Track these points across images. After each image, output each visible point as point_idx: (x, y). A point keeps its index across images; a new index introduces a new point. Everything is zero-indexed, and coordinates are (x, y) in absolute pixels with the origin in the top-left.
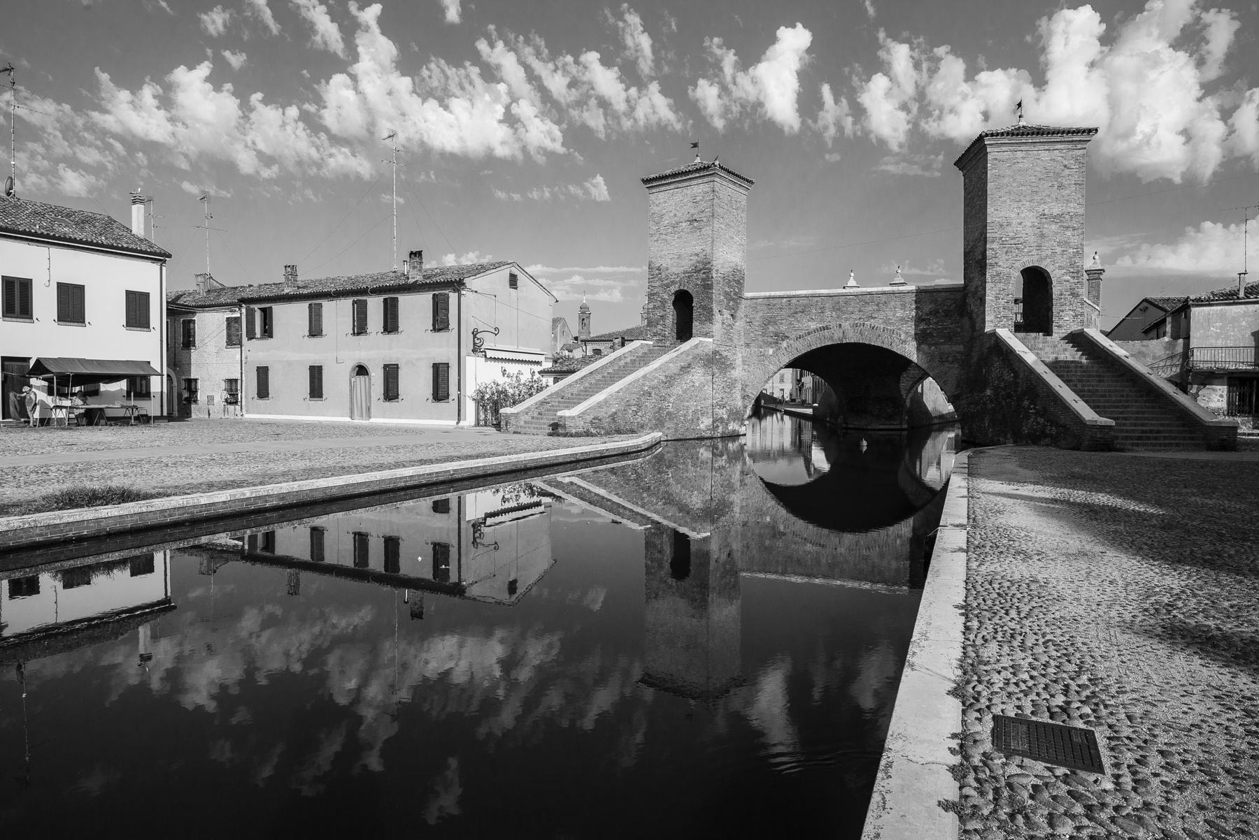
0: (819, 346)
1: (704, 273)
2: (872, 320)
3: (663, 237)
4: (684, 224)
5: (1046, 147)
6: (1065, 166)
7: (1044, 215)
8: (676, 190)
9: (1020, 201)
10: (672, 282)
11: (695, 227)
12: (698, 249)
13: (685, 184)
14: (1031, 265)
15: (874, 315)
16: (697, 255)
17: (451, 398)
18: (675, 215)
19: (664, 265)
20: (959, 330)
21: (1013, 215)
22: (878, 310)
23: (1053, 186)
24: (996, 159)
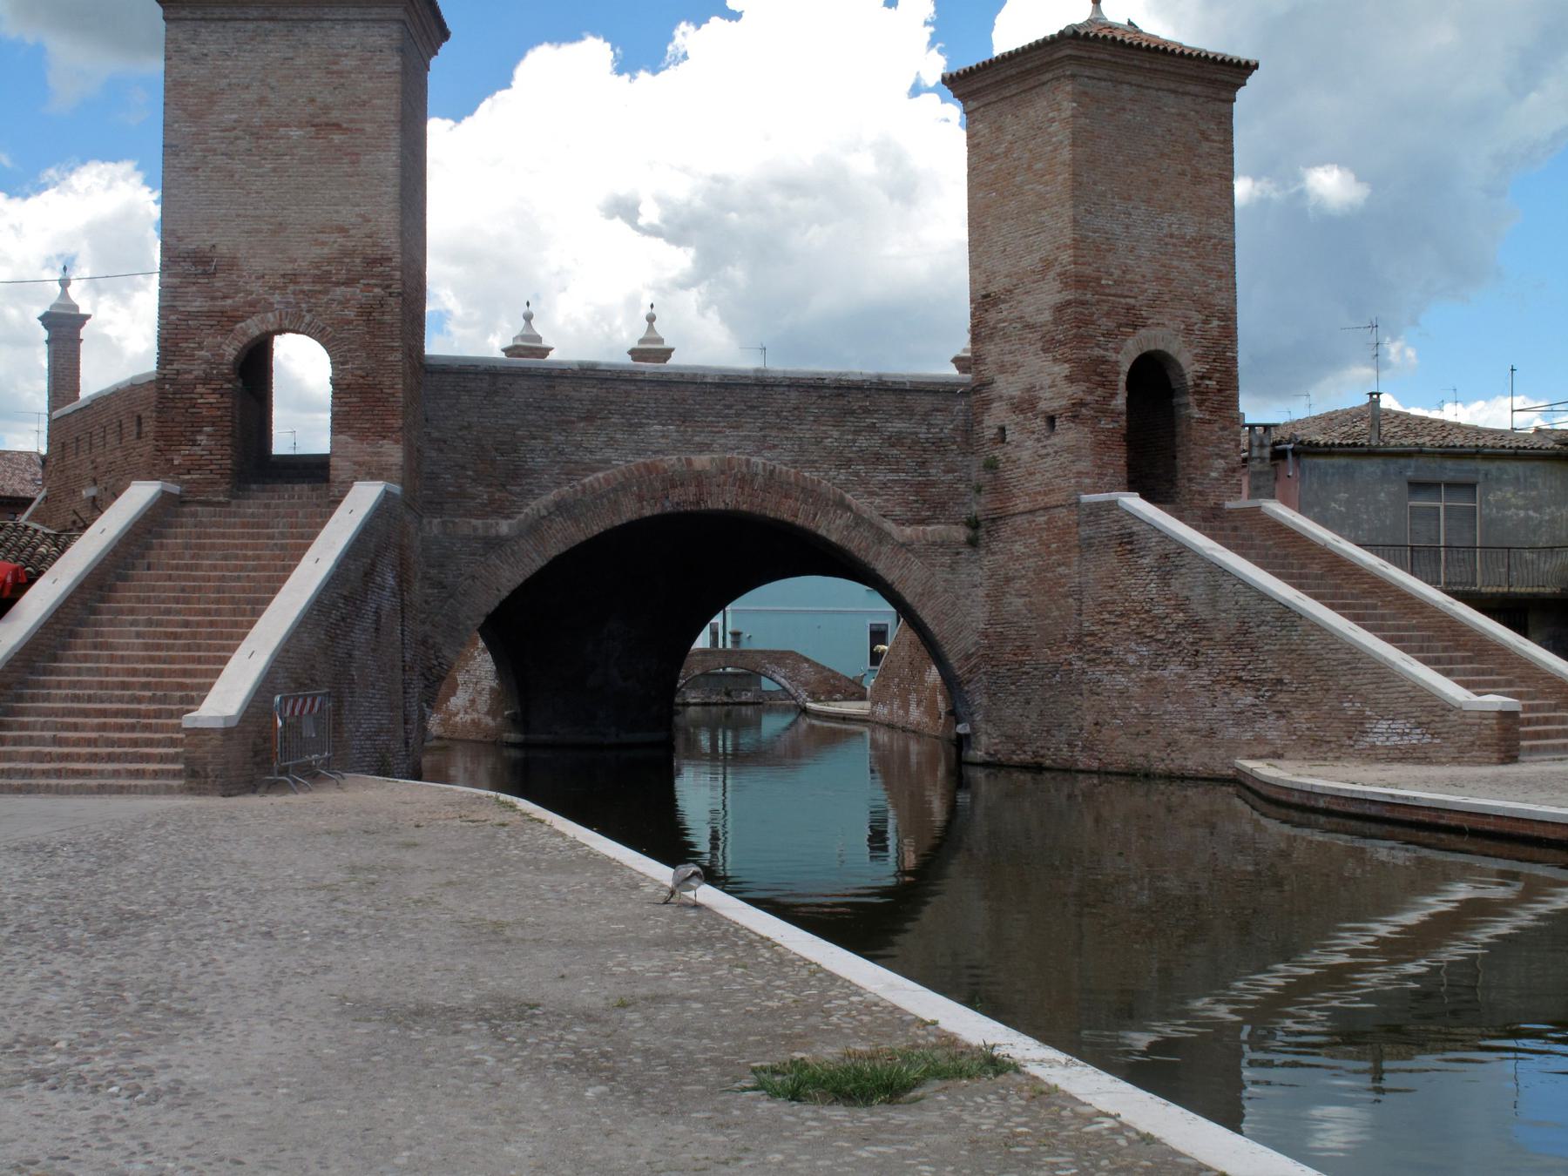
2: (767, 454)
3: (220, 160)
4: (295, 133)
5: (1172, 86)
6: (1202, 133)
7: (1172, 236)
8: (268, 25)
9: (1130, 198)
10: (252, 304)
12: (347, 215)
16: (342, 230)
18: (262, 101)
21: (1118, 230)
23: (1183, 174)
24: (1085, 93)
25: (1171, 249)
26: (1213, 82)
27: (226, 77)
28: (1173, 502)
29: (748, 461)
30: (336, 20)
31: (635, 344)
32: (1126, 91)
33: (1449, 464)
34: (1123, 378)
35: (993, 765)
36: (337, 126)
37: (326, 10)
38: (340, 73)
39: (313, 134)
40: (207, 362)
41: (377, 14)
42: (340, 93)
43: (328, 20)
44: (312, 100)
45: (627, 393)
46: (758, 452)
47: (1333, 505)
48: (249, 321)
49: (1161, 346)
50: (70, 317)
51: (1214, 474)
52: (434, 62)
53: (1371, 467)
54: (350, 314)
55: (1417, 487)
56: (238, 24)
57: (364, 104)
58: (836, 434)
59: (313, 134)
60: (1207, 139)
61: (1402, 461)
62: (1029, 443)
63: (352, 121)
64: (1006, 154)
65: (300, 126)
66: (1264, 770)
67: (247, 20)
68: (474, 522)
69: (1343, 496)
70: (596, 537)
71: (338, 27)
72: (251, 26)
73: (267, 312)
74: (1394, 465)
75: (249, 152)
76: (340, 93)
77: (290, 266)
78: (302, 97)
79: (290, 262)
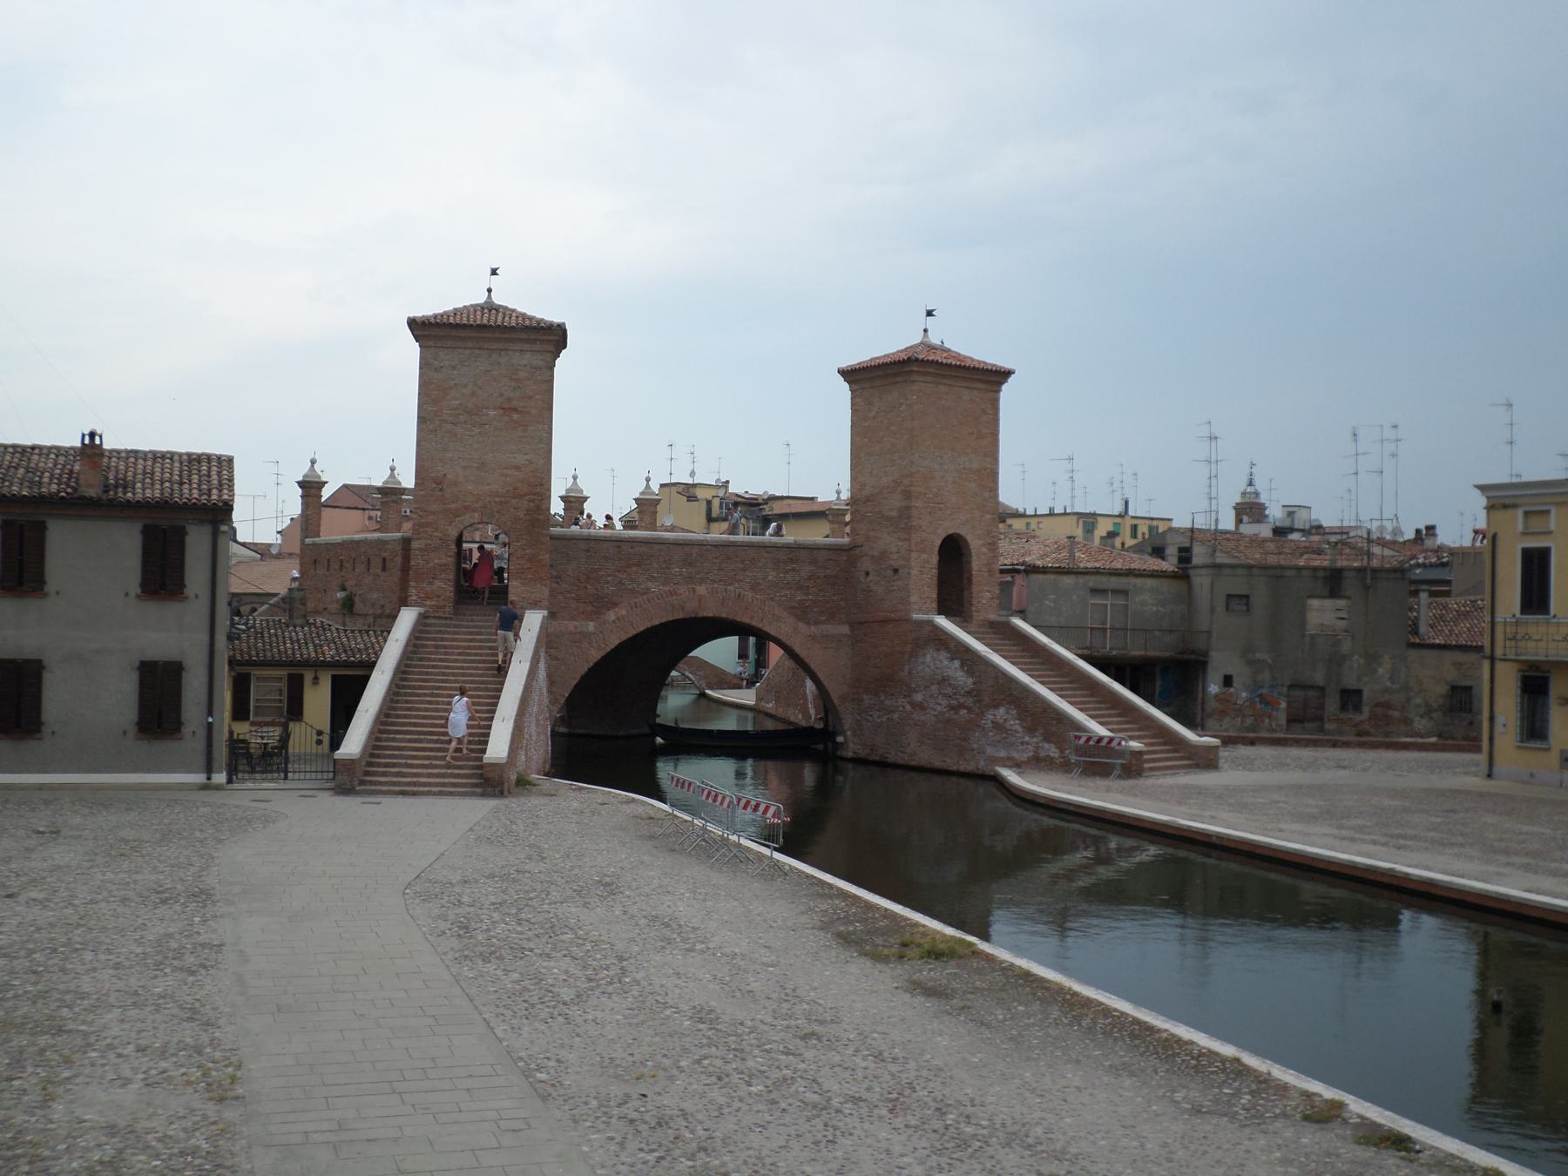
0: (664, 620)
1: (531, 501)
3: (449, 427)
4: (492, 413)
6: (983, 410)
7: (965, 468)
8: (477, 352)
10: (465, 508)
12: (520, 459)
13: (495, 346)
14: (950, 532)
15: (738, 577)
16: (517, 468)
17: (187, 730)
18: (473, 394)
19: (449, 476)
20: (843, 603)
22: (744, 570)
25: (964, 476)
26: (988, 382)
27: (453, 379)
28: (960, 616)
29: (726, 590)
31: (637, 495)
32: (943, 389)
33: (1114, 579)
34: (937, 549)
35: (859, 761)
36: (515, 410)
40: (441, 539)
44: (502, 395)
45: (660, 550)
46: (730, 584)
47: (1047, 602)
48: (463, 517)
49: (958, 531)
50: (318, 483)
51: (984, 601)
52: (558, 361)
53: (1068, 580)
54: (521, 514)
55: (1095, 591)
56: (460, 351)
57: (530, 398)
58: (774, 574)
60: (986, 413)
61: (1088, 577)
62: (883, 583)
63: (524, 407)
64: (874, 418)
65: (495, 409)
66: (1012, 777)
67: (466, 348)
68: (575, 623)
69: (1052, 596)
70: (642, 632)
72: (468, 352)
74: (1082, 580)
75: (466, 422)
77: (487, 487)
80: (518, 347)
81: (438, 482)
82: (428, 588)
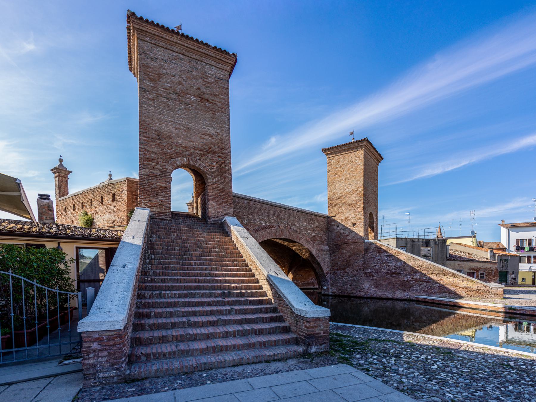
4: (193, 98)
10: (178, 154)
11: (208, 108)
30: (207, 63)
36: (208, 101)
37: (204, 58)
38: (208, 83)
39: (199, 100)
41: (220, 66)
42: (208, 89)
43: (204, 62)
44: (199, 89)
48: (176, 159)
59: (199, 100)
65: (195, 97)
71: (208, 66)
73: (184, 157)
76: (208, 89)
77: (192, 143)
78: (195, 86)
79: (192, 142)
80: (209, 61)
81: (159, 135)
82: (153, 201)
